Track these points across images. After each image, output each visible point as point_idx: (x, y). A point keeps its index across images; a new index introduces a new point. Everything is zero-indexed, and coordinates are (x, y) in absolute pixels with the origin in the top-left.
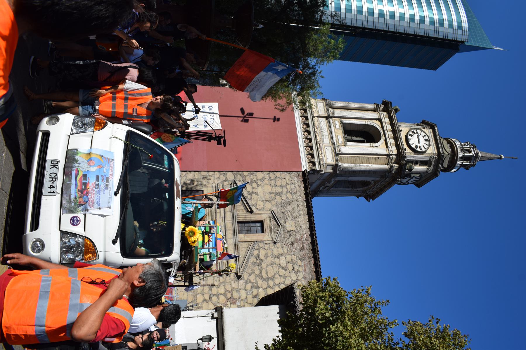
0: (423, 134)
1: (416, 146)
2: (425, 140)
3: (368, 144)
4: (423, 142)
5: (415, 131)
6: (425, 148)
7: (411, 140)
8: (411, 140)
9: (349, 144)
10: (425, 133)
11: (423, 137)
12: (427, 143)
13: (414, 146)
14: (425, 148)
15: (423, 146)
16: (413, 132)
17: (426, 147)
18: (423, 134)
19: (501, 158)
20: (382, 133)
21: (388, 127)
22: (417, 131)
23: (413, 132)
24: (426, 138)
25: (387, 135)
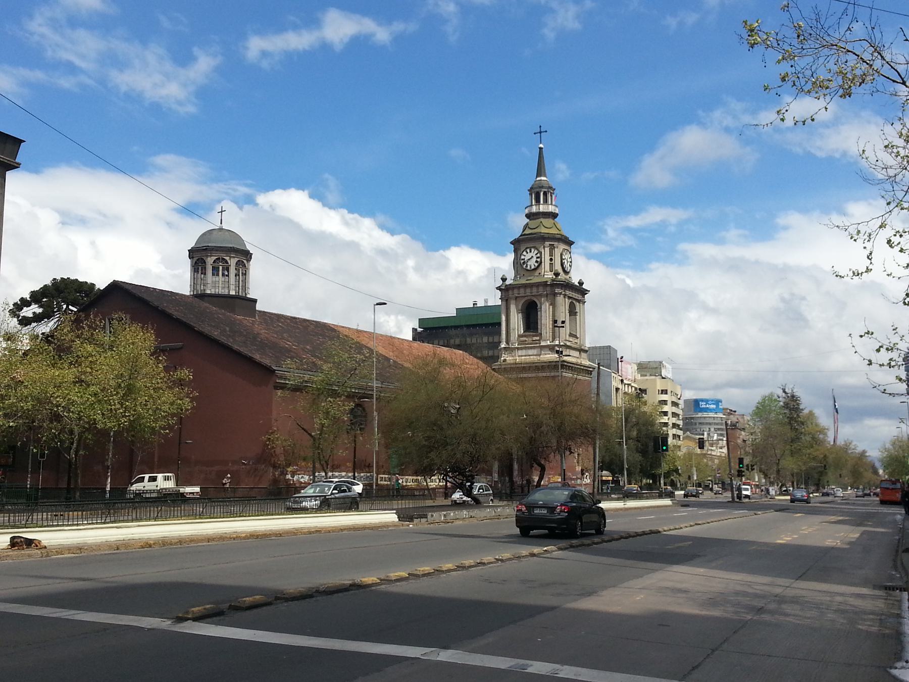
0: (525, 253)
1: (537, 262)
2: (531, 252)
3: (539, 313)
4: (534, 253)
5: (522, 261)
6: (537, 253)
7: (531, 267)
8: (531, 267)
9: (539, 331)
10: (523, 251)
11: (527, 253)
12: (533, 250)
13: (536, 265)
14: (537, 253)
15: (536, 254)
16: (524, 263)
17: (536, 252)
18: (525, 253)
19: (541, 148)
20: (529, 298)
21: (522, 291)
22: (522, 259)
23: (524, 263)
24: (528, 251)
25: (529, 294)
